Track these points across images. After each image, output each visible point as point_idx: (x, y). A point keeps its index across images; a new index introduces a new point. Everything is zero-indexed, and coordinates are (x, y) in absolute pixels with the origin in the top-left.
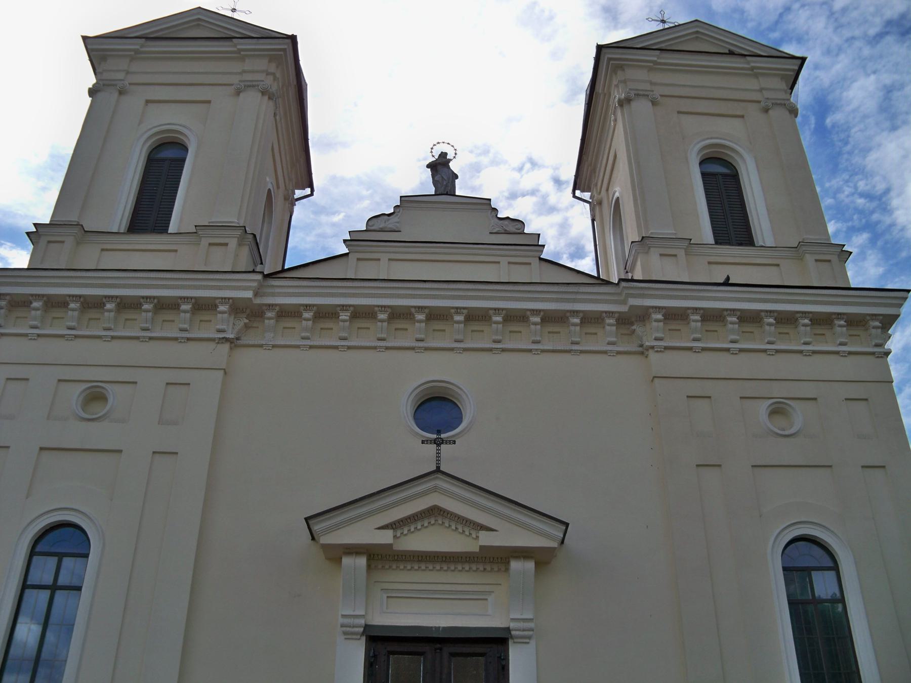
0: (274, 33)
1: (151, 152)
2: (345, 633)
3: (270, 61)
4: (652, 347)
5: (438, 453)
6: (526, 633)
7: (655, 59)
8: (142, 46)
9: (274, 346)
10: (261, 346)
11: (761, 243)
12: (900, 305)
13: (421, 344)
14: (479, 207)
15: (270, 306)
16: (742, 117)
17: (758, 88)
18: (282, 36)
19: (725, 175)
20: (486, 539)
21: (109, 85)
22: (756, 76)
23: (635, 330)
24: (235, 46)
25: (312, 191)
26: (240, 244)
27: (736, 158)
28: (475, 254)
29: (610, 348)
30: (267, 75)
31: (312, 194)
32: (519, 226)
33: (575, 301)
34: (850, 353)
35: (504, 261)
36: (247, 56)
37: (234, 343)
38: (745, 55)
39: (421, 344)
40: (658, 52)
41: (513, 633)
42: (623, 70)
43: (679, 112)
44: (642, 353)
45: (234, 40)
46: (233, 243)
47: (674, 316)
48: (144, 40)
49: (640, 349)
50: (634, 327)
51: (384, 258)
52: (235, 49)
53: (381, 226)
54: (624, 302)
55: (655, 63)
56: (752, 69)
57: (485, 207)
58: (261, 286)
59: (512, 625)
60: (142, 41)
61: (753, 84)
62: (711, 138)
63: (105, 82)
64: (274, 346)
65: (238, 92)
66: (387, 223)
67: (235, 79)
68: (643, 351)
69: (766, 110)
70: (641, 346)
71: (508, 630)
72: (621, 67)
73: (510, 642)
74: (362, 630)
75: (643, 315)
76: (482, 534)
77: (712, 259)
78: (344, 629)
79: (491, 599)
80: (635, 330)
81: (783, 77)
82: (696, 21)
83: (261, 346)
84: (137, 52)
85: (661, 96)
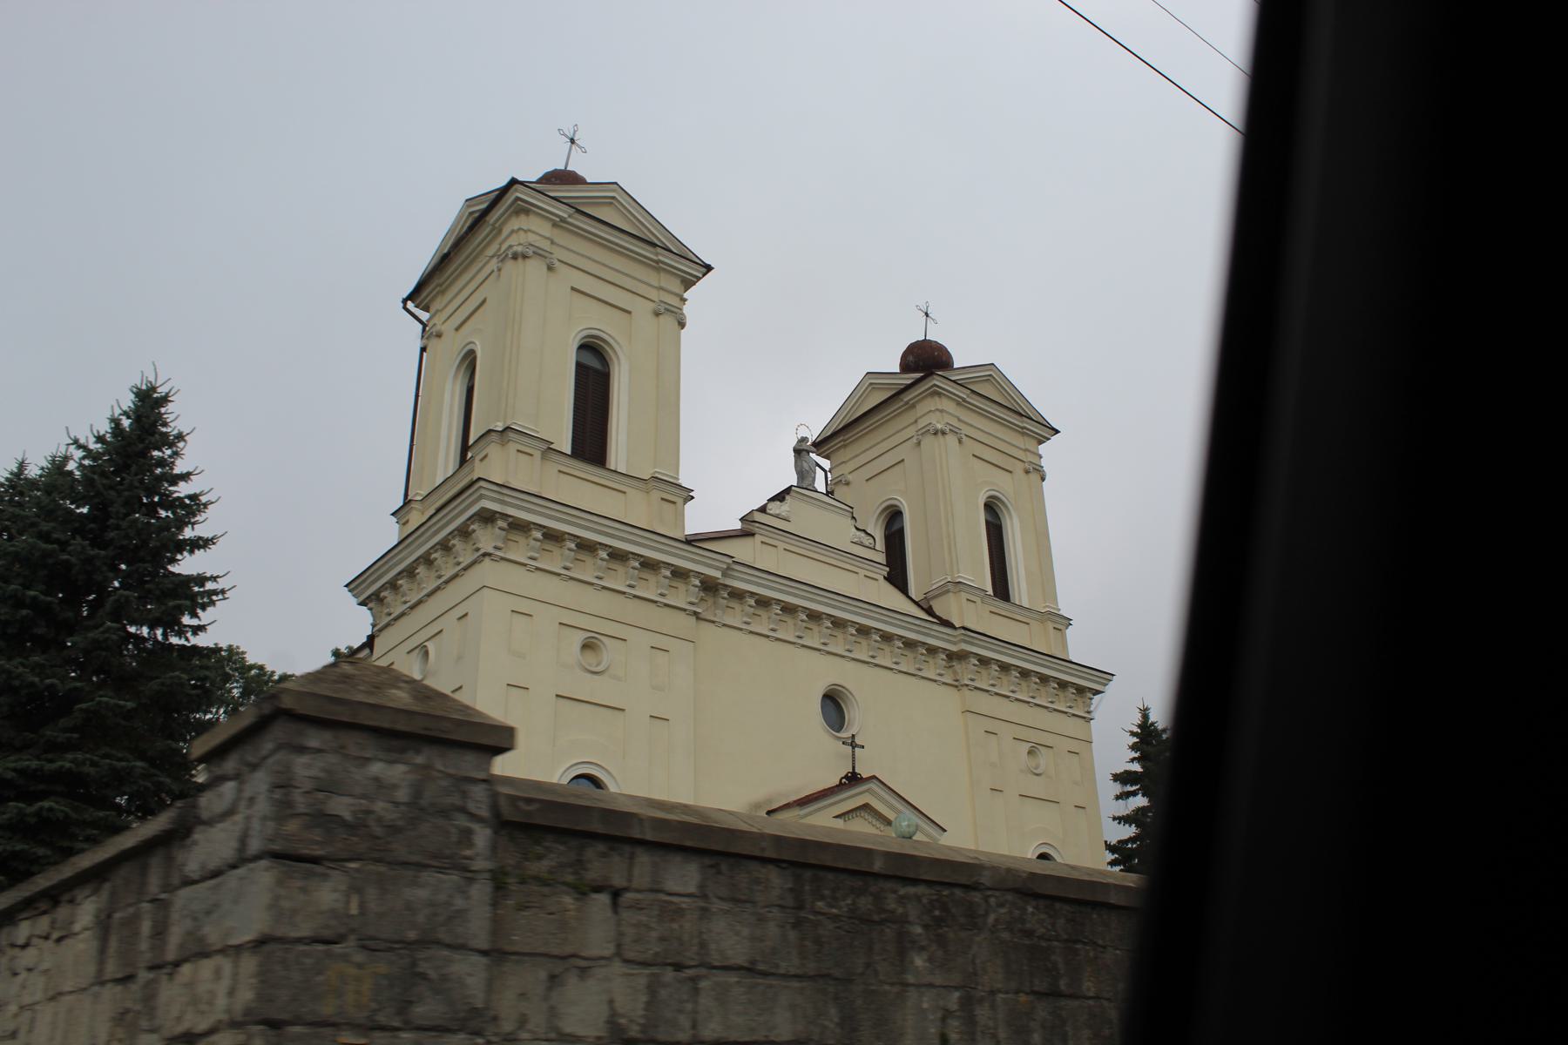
4: (967, 685)
5: (853, 752)
7: (965, 397)
9: (724, 625)
10: (713, 622)
12: (1106, 685)
14: (841, 511)
22: (1023, 434)
24: (657, 254)
32: (871, 541)
34: (1074, 715)
36: (664, 270)
38: (1023, 415)
40: (969, 392)
42: (940, 397)
44: (956, 687)
47: (984, 662)
49: (956, 683)
50: (954, 664)
51: (781, 545)
52: (655, 258)
53: (777, 512)
54: (955, 643)
55: (964, 400)
57: (847, 514)
58: (729, 568)
60: (571, 211)
62: (997, 491)
64: (724, 625)
65: (657, 314)
68: (957, 686)
69: (1027, 472)
70: (957, 681)
72: (939, 394)
75: (961, 656)
77: (994, 610)
82: (993, 364)
83: (713, 622)
84: (563, 220)
85: (966, 435)
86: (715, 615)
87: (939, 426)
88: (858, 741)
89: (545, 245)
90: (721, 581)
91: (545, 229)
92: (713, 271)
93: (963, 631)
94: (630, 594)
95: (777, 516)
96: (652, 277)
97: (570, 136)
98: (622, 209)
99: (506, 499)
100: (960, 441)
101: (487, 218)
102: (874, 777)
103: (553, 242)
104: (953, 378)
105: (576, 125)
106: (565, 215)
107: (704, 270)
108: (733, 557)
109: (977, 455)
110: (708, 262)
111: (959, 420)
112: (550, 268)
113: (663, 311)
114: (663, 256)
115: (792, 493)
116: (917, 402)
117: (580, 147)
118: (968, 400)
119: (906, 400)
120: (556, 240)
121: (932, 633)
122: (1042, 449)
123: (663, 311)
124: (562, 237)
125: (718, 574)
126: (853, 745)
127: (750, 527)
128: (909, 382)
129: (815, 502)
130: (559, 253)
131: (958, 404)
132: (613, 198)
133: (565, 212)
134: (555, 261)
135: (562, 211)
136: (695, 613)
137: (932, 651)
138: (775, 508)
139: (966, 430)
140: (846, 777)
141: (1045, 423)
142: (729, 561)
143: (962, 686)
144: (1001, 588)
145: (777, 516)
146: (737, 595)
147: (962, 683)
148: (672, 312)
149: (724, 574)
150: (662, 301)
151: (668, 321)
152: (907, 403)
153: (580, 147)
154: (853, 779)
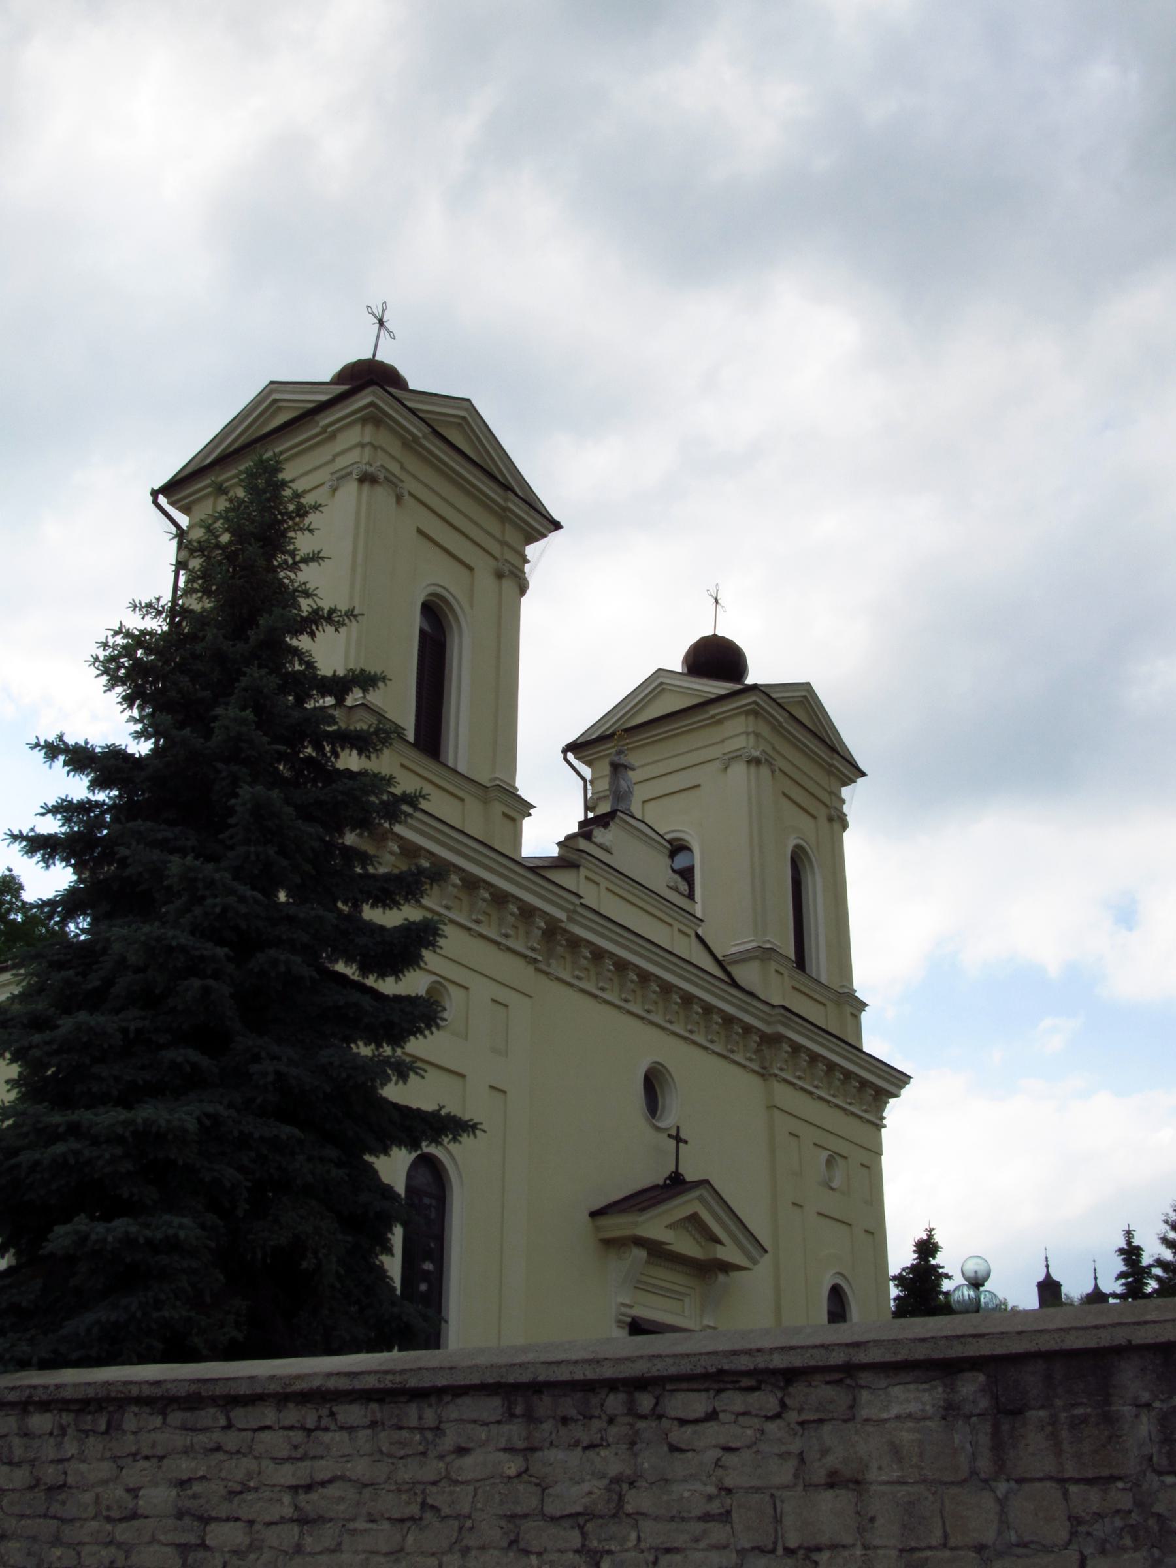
0: (540, 505)
2: (619, 1321)
4: (776, 1076)
8: (424, 437)
13: (623, 1004)
18: (547, 515)
21: (391, 482)
23: (762, 1050)
24: (506, 500)
27: (806, 863)
28: (639, 897)
29: (748, 1063)
32: (687, 887)
33: (746, 1011)
35: (677, 925)
39: (668, 1026)
40: (787, 715)
44: (763, 1075)
45: (510, 492)
48: (430, 429)
51: (604, 884)
54: (768, 1023)
55: (780, 723)
56: (831, 765)
60: (427, 430)
62: (807, 844)
68: (764, 1075)
72: (756, 714)
74: (629, 1320)
76: (719, 1246)
77: (798, 986)
78: (621, 1317)
79: (687, 1300)
80: (762, 1050)
84: (415, 439)
86: (549, 965)
87: (756, 754)
88: (683, 1135)
89: (394, 468)
90: (563, 925)
92: (562, 530)
93: (782, 1011)
95: (600, 846)
96: (494, 526)
97: (379, 315)
98: (471, 434)
100: (773, 772)
101: (317, 418)
102: (705, 1183)
103: (403, 467)
105: (385, 302)
106: (419, 434)
107: (552, 527)
108: (581, 897)
110: (556, 517)
111: (774, 749)
112: (399, 499)
113: (507, 573)
114: (515, 504)
115: (617, 820)
116: (725, 718)
117: (389, 332)
118: (785, 725)
119: (712, 713)
121: (751, 1009)
122: (846, 792)
123: (507, 573)
124: (413, 464)
125: (561, 915)
126: (678, 1139)
127: (574, 857)
128: (723, 692)
129: (636, 833)
130: (410, 485)
133: (420, 430)
134: (406, 494)
136: (535, 961)
137: (748, 1029)
138: (599, 835)
140: (670, 1177)
141: (849, 758)
142: (577, 901)
143: (770, 1075)
144: (800, 962)
145: (600, 846)
146: (575, 943)
147: (772, 1072)
149: (570, 919)
150: (506, 560)
151: (508, 585)
152: (713, 717)
153: (389, 332)
154: (676, 1184)
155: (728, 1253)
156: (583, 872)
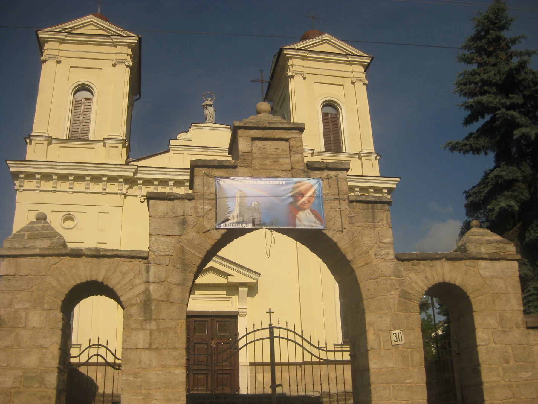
1: (75, 93)
3: (128, 48)
6: (244, 313)
11: (344, 151)
15: (140, 179)
16: (343, 85)
17: (351, 70)
19: (332, 114)
20: (231, 279)
22: (351, 64)
25: (140, 95)
26: (123, 147)
30: (127, 55)
31: (140, 98)
37: (125, 195)
40: (308, 52)
41: (239, 313)
43: (315, 82)
46: (120, 146)
51: (185, 153)
53: (183, 138)
55: (306, 57)
56: (349, 61)
59: (240, 310)
61: (349, 68)
63: (50, 56)
66: (186, 136)
67: (114, 57)
69: (353, 83)
71: (238, 312)
72: (291, 58)
73: (239, 316)
81: (363, 66)
84: (63, 39)
91: (56, 45)
94: (87, 192)
95: (184, 140)
99: (19, 165)
104: (296, 48)
106: (64, 37)
109: (316, 81)
118: (308, 55)
120: (61, 49)
124: (63, 47)
131: (304, 60)
132: (92, 21)
135: (62, 36)
139: (306, 70)
142: (136, 167)
145: (184, 140)
148: (122, 62)
155: (238, 277)
156: (172, 152)
